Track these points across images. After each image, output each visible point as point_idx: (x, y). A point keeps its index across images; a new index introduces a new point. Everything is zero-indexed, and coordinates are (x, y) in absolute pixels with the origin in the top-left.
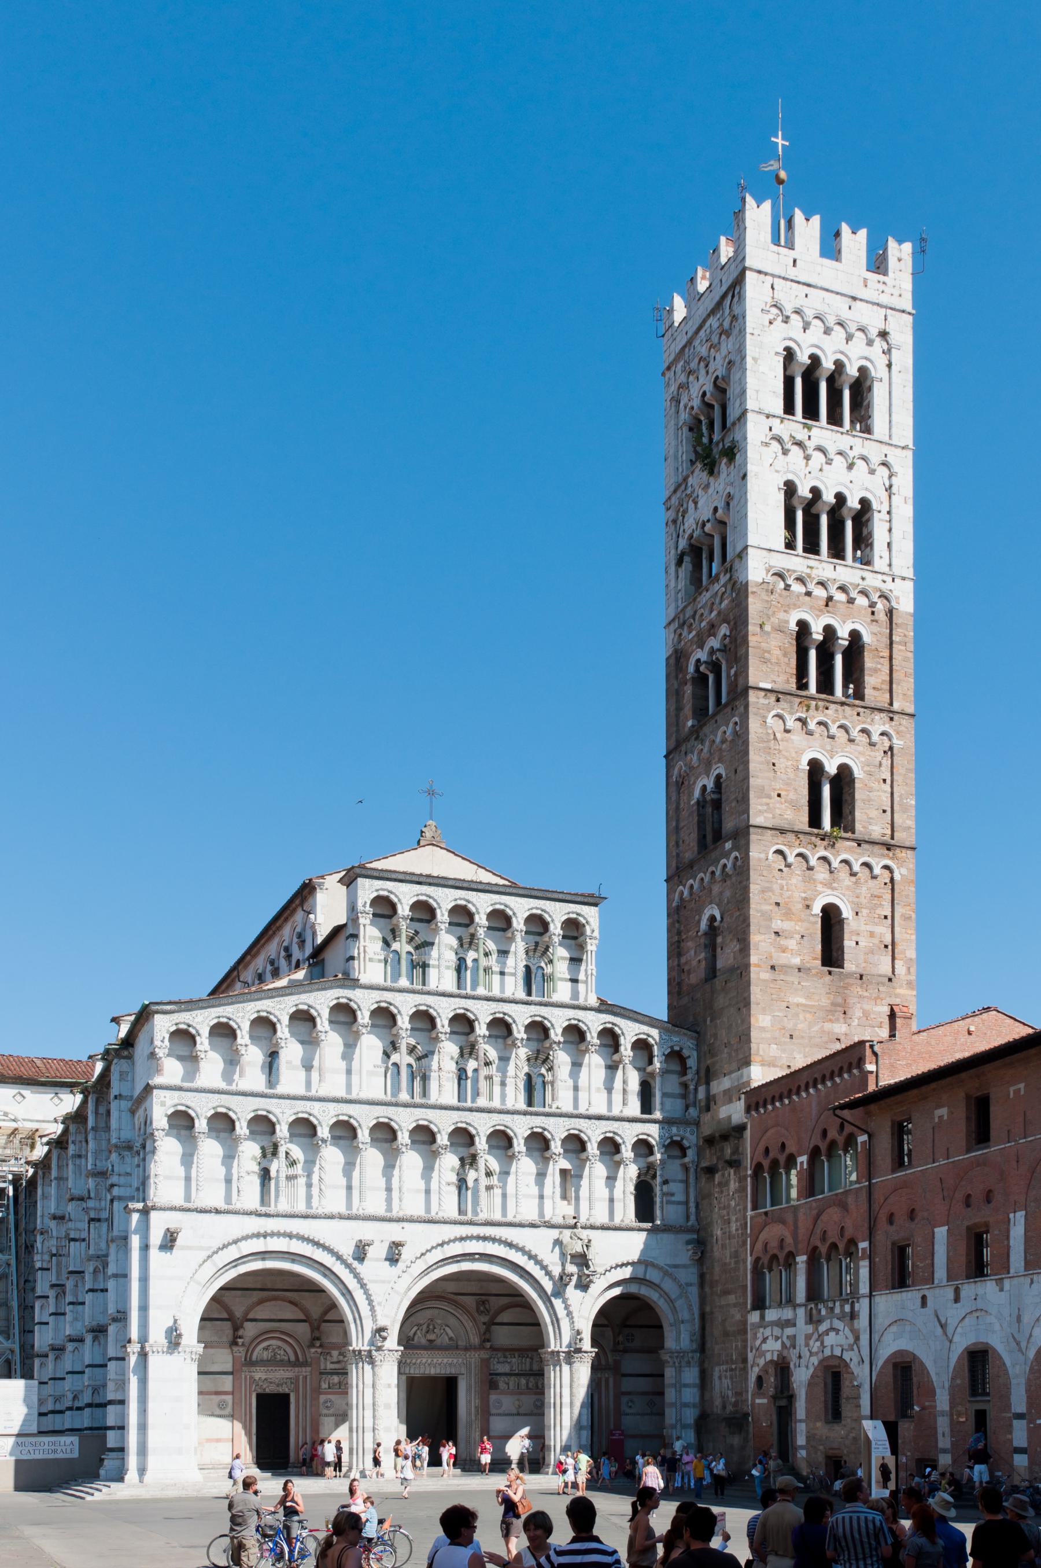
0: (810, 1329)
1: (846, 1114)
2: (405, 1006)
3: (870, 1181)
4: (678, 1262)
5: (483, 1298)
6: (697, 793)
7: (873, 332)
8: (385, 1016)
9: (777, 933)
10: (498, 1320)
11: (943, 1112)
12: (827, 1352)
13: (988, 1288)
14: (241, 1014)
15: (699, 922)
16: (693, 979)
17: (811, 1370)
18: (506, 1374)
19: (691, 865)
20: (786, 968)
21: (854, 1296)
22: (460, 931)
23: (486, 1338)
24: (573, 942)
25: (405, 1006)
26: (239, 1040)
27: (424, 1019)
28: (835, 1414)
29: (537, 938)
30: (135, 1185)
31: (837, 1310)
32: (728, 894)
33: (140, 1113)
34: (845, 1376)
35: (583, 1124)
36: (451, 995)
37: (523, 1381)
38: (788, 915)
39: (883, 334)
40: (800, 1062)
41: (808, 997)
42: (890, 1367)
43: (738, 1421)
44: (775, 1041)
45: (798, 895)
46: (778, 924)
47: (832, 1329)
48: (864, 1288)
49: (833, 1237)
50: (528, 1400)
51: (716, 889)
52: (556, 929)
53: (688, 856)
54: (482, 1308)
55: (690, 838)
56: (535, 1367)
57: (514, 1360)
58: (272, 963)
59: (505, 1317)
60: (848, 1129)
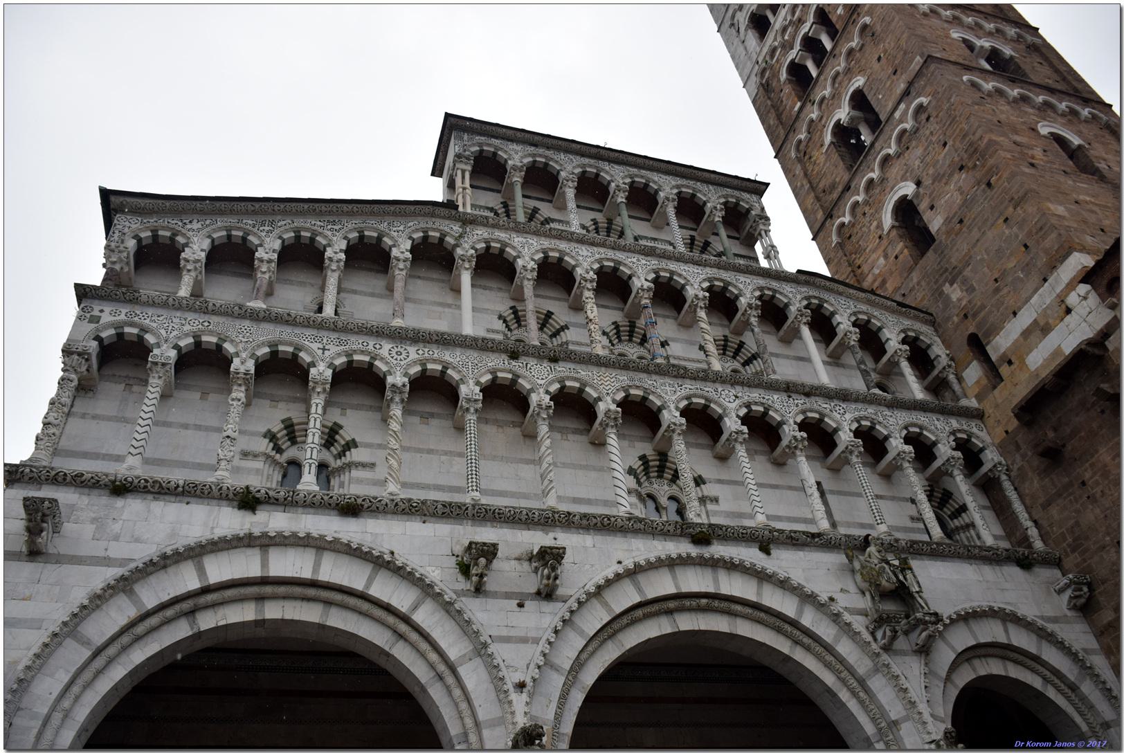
14: (267, 228)
15: (880, 226)
22: (593, 215)
29: (693, 233)
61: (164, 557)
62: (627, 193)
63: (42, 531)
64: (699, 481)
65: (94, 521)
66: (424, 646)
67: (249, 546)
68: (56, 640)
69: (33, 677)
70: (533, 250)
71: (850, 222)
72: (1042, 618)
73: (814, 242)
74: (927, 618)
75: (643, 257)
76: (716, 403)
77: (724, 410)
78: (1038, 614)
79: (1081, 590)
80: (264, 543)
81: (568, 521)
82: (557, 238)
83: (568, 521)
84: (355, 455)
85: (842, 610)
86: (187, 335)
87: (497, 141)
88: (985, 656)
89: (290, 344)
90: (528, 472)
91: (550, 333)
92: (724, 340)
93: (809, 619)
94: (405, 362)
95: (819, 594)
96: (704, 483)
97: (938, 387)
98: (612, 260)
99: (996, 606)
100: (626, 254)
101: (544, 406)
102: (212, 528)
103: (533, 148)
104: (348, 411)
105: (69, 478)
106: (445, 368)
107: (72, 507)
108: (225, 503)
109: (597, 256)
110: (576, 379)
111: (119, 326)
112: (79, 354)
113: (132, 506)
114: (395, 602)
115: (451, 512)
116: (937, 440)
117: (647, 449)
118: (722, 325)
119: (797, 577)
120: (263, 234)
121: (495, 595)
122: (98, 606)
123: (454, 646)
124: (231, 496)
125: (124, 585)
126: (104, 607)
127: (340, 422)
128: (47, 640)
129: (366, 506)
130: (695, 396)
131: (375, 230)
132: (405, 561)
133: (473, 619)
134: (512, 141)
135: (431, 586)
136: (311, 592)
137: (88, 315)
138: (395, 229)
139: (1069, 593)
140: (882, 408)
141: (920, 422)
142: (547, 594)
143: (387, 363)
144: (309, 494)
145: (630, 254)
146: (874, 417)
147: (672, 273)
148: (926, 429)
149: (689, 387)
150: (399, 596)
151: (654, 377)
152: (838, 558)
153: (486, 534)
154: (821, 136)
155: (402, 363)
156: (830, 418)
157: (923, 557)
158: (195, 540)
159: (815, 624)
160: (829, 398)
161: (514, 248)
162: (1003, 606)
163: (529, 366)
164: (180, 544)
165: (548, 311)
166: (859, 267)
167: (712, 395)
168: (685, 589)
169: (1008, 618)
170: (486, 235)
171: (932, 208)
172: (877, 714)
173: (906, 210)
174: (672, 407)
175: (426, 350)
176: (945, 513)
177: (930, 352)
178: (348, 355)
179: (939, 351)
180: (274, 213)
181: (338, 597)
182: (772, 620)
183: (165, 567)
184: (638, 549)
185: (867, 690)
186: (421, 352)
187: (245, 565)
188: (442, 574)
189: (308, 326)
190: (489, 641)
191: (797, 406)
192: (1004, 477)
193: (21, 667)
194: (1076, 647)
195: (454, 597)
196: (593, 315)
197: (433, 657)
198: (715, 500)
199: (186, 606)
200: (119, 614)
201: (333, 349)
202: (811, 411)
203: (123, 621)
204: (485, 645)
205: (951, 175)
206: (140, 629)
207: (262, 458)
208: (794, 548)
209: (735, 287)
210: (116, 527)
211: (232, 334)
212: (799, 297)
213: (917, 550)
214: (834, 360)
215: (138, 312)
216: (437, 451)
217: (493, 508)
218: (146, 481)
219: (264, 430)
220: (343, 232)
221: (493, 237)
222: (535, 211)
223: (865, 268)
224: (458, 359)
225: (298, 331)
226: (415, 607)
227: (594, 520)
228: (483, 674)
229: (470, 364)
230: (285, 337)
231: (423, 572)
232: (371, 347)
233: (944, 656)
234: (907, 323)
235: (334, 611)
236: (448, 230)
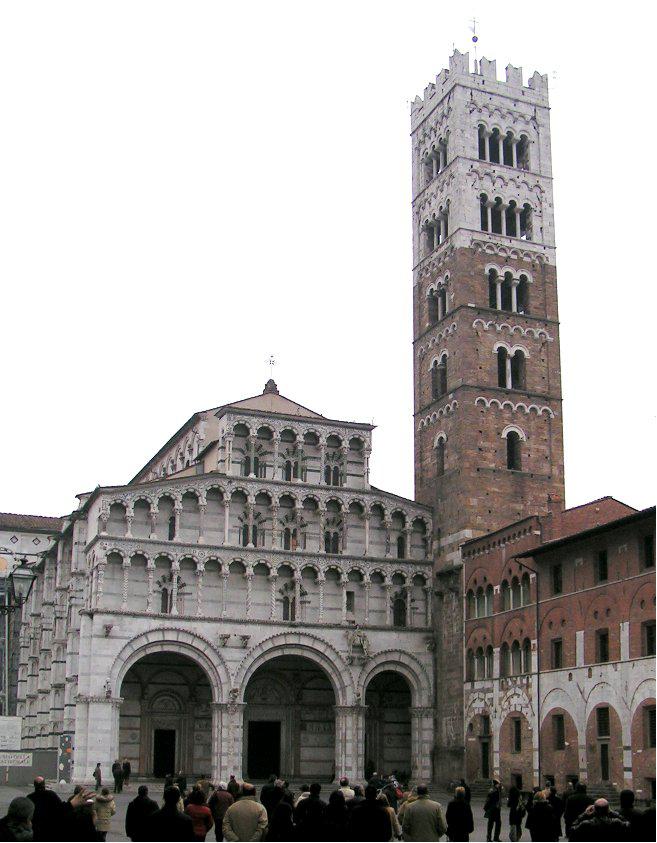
0: (502, 693)
1: (523, 561)
2: (252, 490)
3: (538, 600)
4: (420, 650)
6: (432, 366)
7: (528, 118)
8: (240, 495)
9: (480, 449)
10: (307, 686)
11: (580, 561)
12: (513, 709)
13: (608, 669)
16: (430, 475)
17: (503, 720)
19: (429, 407)
20: (487, 470)
21: (528, 673)
22: (287, 445)
23: (299, 697)
25: (252, 490)
26: (152, 510)
27: (264, 497)
28: (518, 747)
29: (334, 450)
30: (85, 598)
31: (518, 682)
32: (450, 424)
33: (91, 553)
34: (523, 725)
36: (282, 484)
37: (322, 726)
38: (487, 438)
39: (534, 118)
40: (495, 527)
41: (500, 487)
42: (550, 718)
43: (458, 753)
44: (479, 514)
45: (493, 426)
46: (482, 444)
47: (515, 694)
48: (534, 669)
49: (517, 636)
50: (325, 738)
51: (444, 421)
52: (345, 444)
53: (427, 402)
55: (429, 391)
56: (330, 717)
58: (172, 462)
60: (524, 570)
64: (303, 594)
80: (163, 630)
81: (253, 622)
83: (253, 622)
84: (186, 589)
90: (242, 594)
97: (425, 540)
107: (112, 621)
113: (127, 619)
115: (216, 620)
117: (286, 580)
134: (252, 415)
142: (244, 647)
149: (307, 560)
150: (201, 646)
153: (227, 629)
169: (401, 652)
172: (342, 683)
179: (429, 527)
188: (216, 643)
213: (375, 629)
214: (382, 527)
233: (373, 664)
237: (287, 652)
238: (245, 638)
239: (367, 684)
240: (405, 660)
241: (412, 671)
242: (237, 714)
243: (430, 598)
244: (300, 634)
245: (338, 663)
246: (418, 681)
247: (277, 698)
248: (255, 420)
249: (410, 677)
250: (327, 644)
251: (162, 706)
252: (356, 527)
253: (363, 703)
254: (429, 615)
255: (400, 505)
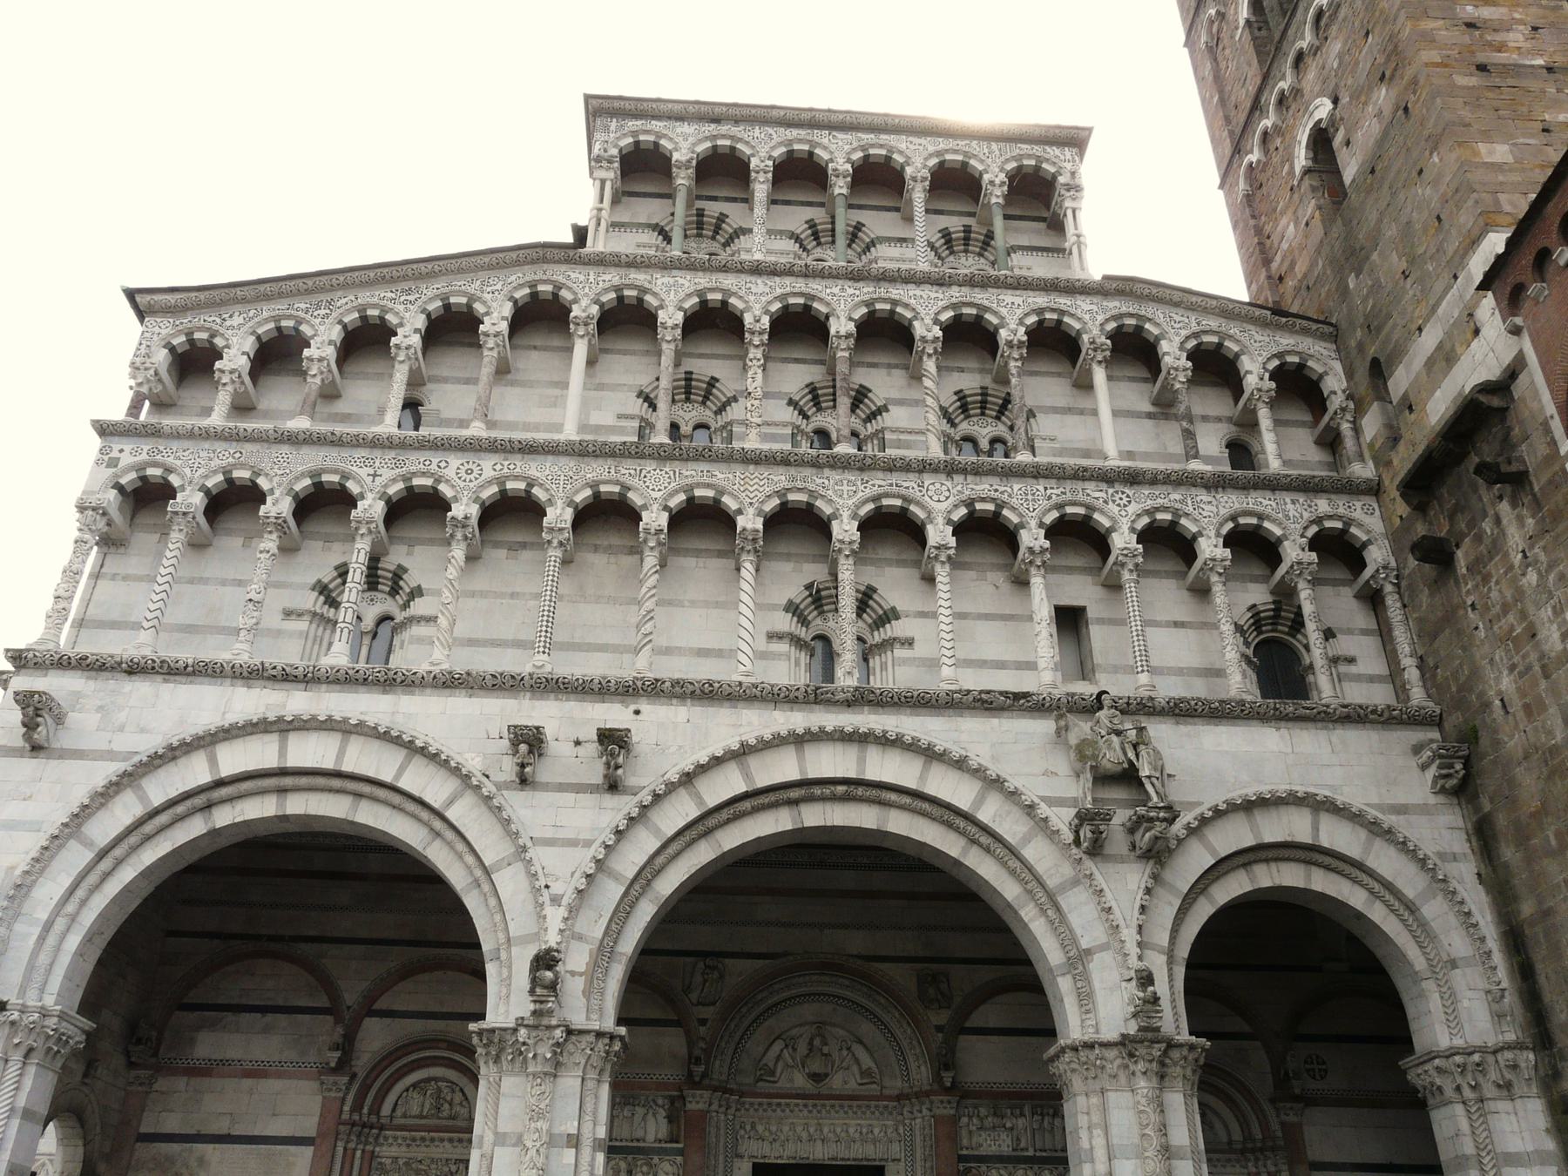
5: (934, 966)
9: (1470, 25)
10: (975, 1020)
14: (322, 312)
18: (1001, 1159)
23: (945, 1061)
24: (1042, 225)
35: (1094, 492)
54: (931, 991)
57: (1021, 1122)
59: (988, 1015)
61: (171, 748)
62: (849, 179)
63: (38, 726)
65: (100, 708)
66: (460, 846)
67: (266, 731)
68: (57, 842)
69: (34, 882)
70: (682, 295)
71: (1259, 161)
72: (1379, 807)
73: (1221, 192)
74: (1152, 814)
75: (850, 283)
76: (918, 503)
77: (929, 513)
78: (1376, 801)
79: (1451, 766)
80: (283, 727)
82: (721, 271)
85: (1037, 800)
86: (215, 472)
87: (659, 124)
88: (1277, 860)
89: (335, 471)
91: (715, 409)
92: (982, 394)
93: (991, 812)
94: (476, 483)
95: (1008, 778)
96: (897, 618)
98: (801, 294)
99: (1300, 790)
100: (824, 282)
101: (653, 531)
102: (224, 713)
103: (713, 126)
104: (418, 549)
105: (73, 661)
106: (530, 485)
107: (77, 695)
108: (240, 682)
109: (779, 291)
110: (708, 486)
111: (141, 467)
112: (94, 509)
113: (141, 688)
114: (428, 799)
116: (1284, 535)
118: (981, 371)
119: (980, 755)
120: (318, 321)
121: (546, 787)
122: (102, 805)
123: (491, 846)
124: (245, 674)
125: (127, 780)
126: (110, 805)
127: (405, 564)
128: (45, 844)
129: (399, 680)
130: (887, 495)
131: (464, 294)
132: (440, 747)
133: (514, 817)
135: (468, 777)
136: (336, 783)
137: (106, 458)
138: (489, 289)
139: (1432, 771)
140: (1194, 491)
141: (1259, 509)
143: (453, 486)
144: (332, 669)
145: (829, 282)
146: (1178, 506)
147: (895, 303)
148: (1268, 518)
151: (827, 472)
152: (1044, 726)
154: (1236, 13)
155: (471, 485)
156: (1102, 512)
157: (1196, 719)
158: (204, 728)
159: (997, 819)
160: (1107, 482)
161: (655, 294)
162: (1312, 790)
163: (644, 472)
164: (187, 733)
165: (712, 378)
166: (1269, 237)
167: (915, 493)
168: (813, 774)
170: (616, 281)
171: (1348, 143)
172: (1067, 938)
173: (1321, 140)
174: (846, 514)
175: (506, 463)
176: (1298, 641)
177: (1322, 386)
178: (406, 478)
179: (1335, 383)
180: (332, 288)
181: (366, 789)
182: (936, 811)
183: (174, 758)
184: (750, 724)
185: (1058, 909)
186: (498, 467)
187: (257, 754)
189: (358, 446)
190: (529, 844)
191: (1050, 498)
192: (1389, 588)
193: (18, 872)
194: (1428, 848)
195: (494, 789)
196: (754, 385)
197: (470, 859)
198: (909, 642)
199: (198, 801)
200: (125, 811)
201: (387, 474)
202: (1074, 504)
203: (128, 821)
204: (524, 849)
205: (1370, 89)
206: (148, 828)
207: (307, 618)
208: (987, 713)
209: (995, 313)
210: (122, 717)
211: (265, 465)
212: (1100, 318)
213: (1181, 711)
215: (161, 448)
216: (524, 594)
217: (555, 677)
218: (153, 661)
219: (313, 581)
220: (419, 303)
221: (627, 282)
222: (722, 218)
223: (1275, 238)
224: (547, 472)
225: (345, 453)
226: (450, 802)
227: (691, 687)
228: (523, 882)
229: (562, 478)
230: (329, 463)
231: (460, 760)
232: (434, 467)
233: (1194, 861)
234: (1286, 341)
235: (365, 805)
236: (564, 281)
237: (815, 816)
238: (613, 741)
239: (1183, 951)
240: (1338, 836)
241: (1386, 889)
242: (570, 1083)
243: (1392, 602)
244: (860, 739)
245: (1039, 854)
246: (1423, 932)
247: (866, 1073)
248: (686, 128)
249: (1378, 914)
250: (979, 773)
251: (415, 1104)
252: (1068, 410)
253: (1173, 1020)
254: (1408, 662)
255: (1213, 323)
